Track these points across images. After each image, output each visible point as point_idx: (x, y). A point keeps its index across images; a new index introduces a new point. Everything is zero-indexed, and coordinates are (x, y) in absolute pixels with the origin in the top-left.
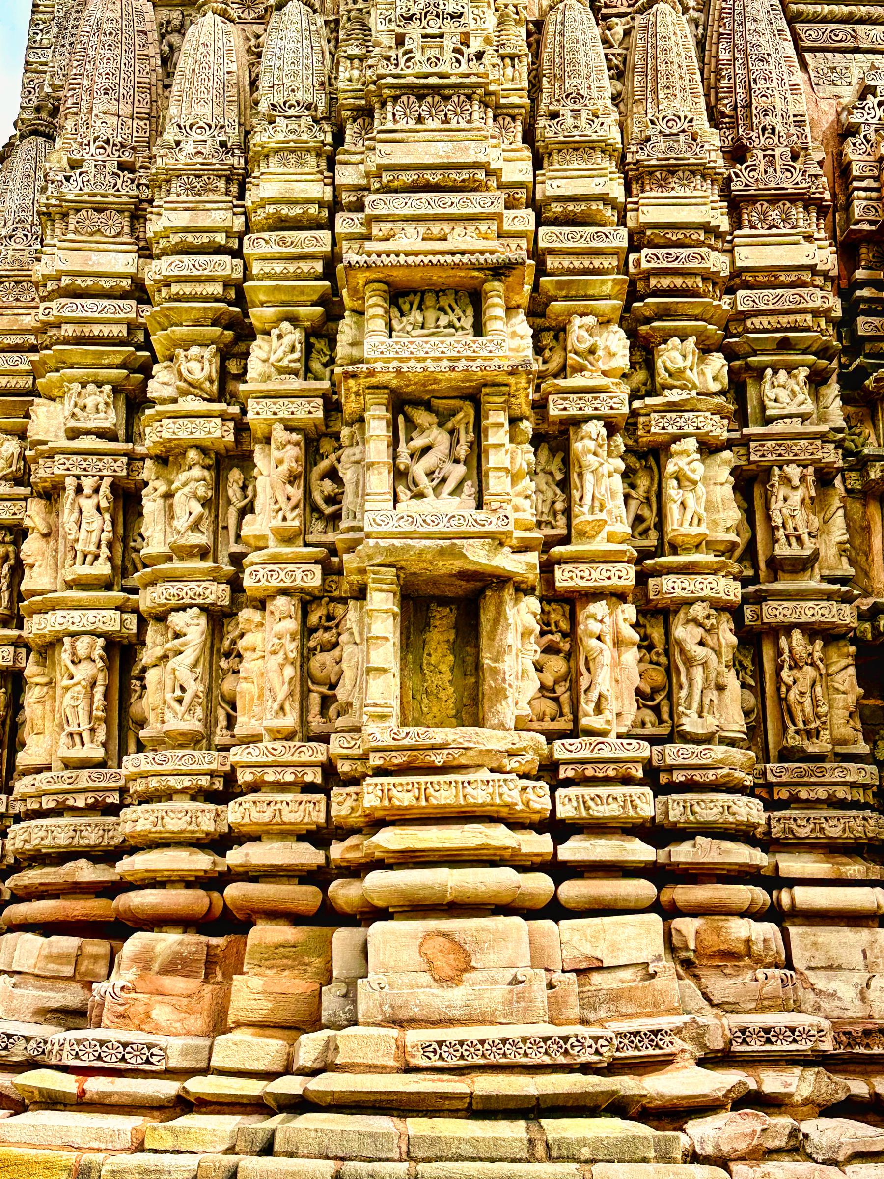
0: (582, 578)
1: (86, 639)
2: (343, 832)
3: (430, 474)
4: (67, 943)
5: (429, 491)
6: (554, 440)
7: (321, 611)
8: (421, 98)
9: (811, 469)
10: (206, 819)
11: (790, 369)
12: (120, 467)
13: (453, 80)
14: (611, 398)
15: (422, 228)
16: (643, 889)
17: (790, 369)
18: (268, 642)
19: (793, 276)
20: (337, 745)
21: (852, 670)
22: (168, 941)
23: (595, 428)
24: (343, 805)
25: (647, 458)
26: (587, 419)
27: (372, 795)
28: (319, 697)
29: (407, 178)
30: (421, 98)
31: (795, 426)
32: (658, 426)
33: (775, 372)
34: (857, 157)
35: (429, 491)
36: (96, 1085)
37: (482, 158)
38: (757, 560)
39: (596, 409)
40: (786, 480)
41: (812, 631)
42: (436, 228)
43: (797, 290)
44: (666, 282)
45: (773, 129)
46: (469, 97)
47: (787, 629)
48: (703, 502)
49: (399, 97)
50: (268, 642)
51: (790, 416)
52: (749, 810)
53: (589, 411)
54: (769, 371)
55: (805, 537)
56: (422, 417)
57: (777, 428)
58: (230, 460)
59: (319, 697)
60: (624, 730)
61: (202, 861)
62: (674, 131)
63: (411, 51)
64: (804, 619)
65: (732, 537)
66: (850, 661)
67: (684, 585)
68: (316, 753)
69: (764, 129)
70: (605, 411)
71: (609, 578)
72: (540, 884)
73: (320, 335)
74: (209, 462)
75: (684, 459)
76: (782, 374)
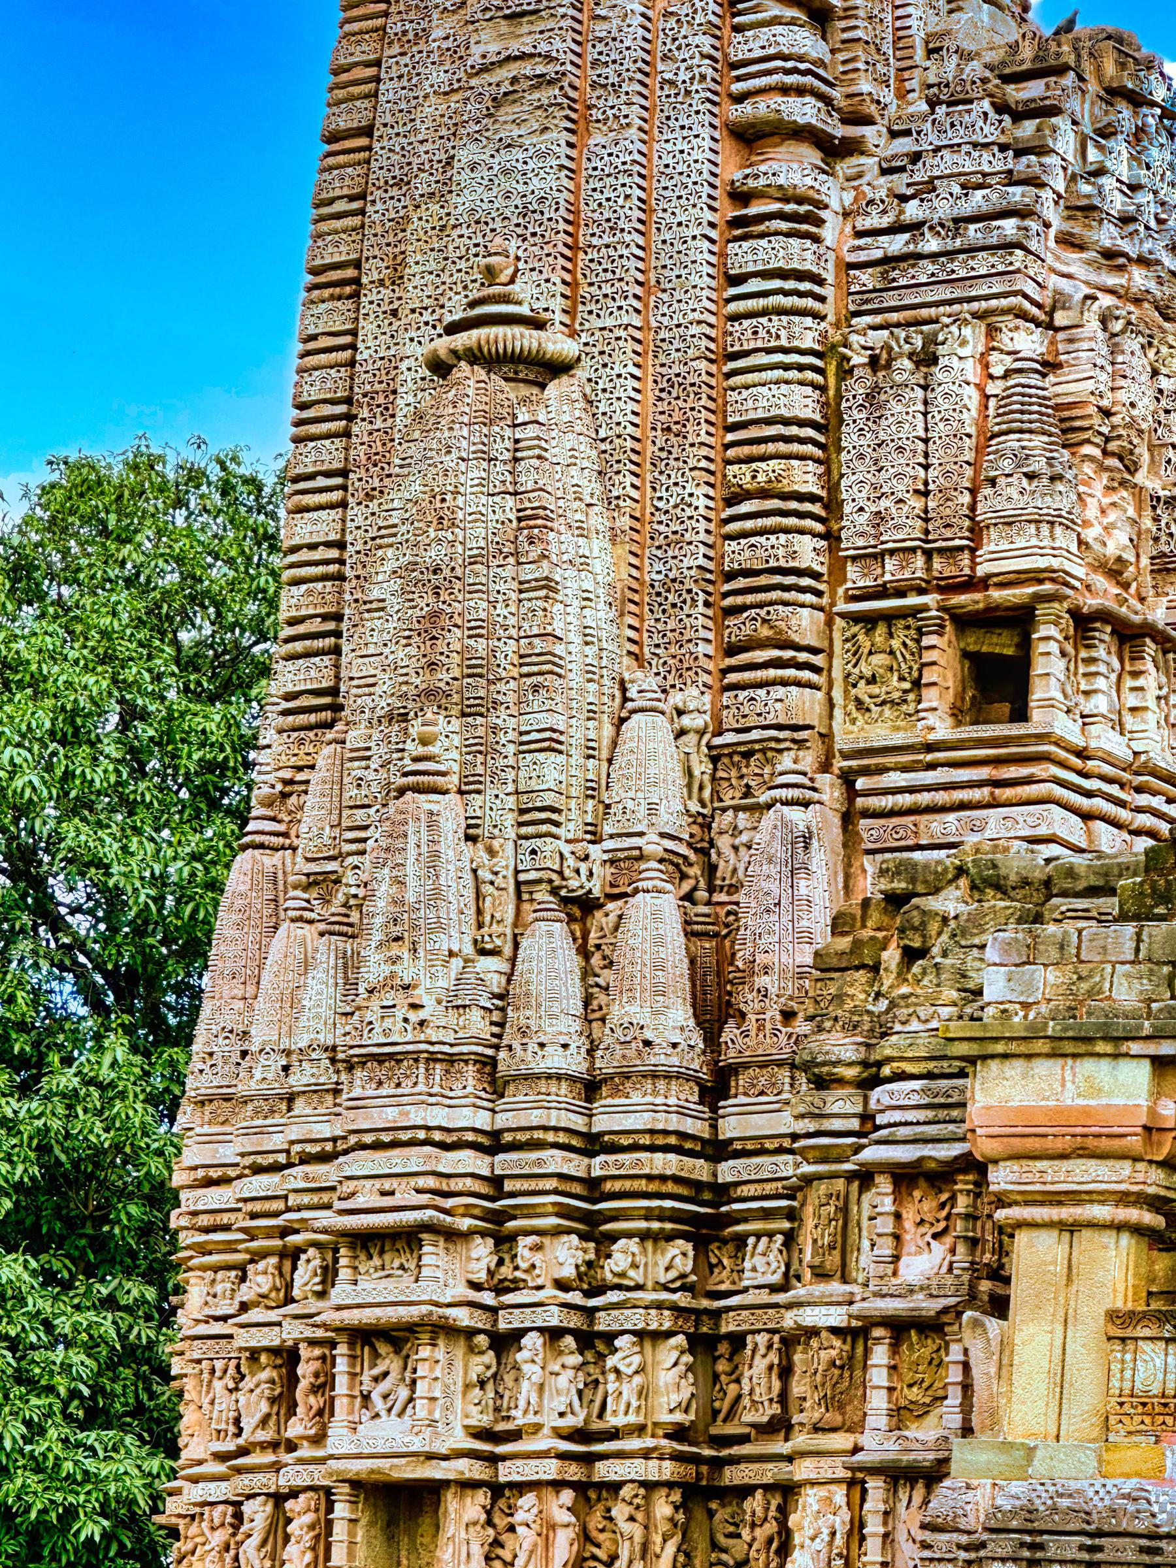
1: (221, 1508)
3: (385, 1397)
5: (383, 1413)
8: (381, 1062)
9: (776, 1338)
15: (378, 1184)
17: (771, 1235)
30: (381, 1062)
32: (603, 1323)
35: (383, 1413)
42: (387, 1185)
46: (416, 1060)
47: (746, 1491)
53: (528, 1324)
54: (751, 1241)
56: (383, 1348)
65: (678, 1417)
74: (279, 1362)
76: (764, 1240)
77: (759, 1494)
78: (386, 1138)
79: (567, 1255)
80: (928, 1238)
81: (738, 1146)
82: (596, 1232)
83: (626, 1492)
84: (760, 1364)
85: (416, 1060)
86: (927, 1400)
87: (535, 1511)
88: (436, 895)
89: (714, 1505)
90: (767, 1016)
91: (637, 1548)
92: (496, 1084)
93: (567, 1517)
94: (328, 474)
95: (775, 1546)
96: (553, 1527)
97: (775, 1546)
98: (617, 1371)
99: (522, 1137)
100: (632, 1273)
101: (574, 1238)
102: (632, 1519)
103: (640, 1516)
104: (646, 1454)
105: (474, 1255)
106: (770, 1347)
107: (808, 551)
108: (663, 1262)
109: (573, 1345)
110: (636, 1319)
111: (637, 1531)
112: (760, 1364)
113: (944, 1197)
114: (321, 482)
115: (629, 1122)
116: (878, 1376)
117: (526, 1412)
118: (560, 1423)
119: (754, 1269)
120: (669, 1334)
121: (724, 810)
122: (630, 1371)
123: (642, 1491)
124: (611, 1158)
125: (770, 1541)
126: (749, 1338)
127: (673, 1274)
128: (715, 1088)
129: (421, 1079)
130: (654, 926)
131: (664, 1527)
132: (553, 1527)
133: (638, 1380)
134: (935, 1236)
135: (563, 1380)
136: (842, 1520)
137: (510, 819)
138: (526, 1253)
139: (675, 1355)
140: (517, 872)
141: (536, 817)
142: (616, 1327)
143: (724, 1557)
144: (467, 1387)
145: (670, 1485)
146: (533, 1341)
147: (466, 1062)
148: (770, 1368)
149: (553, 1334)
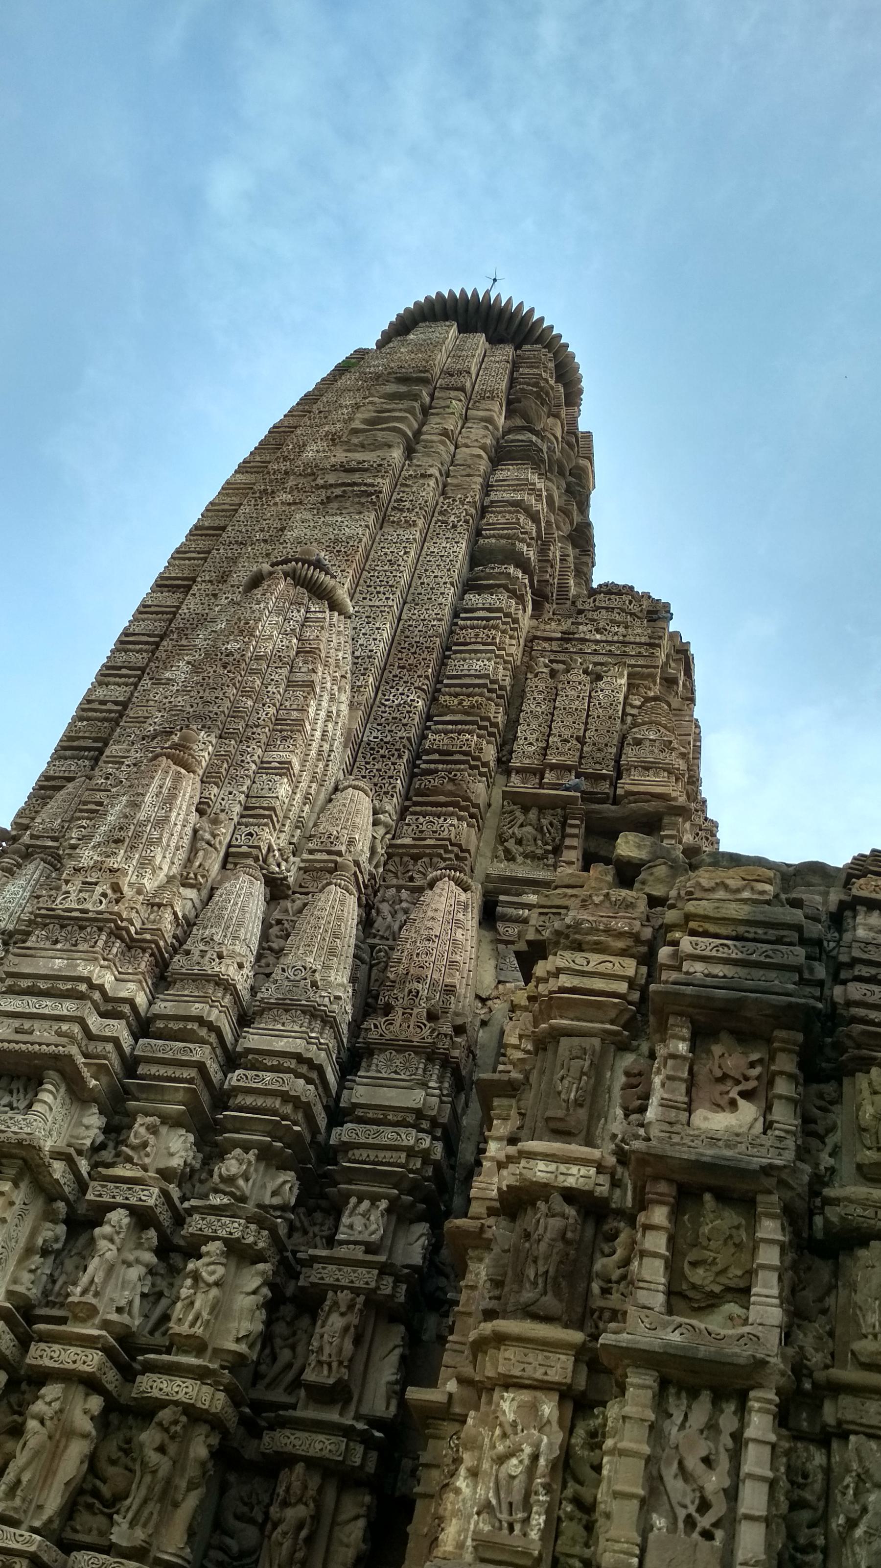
0: (52, 1358)
9: (362, 1298)
11: (375, 1199)
13: (90, 915)
14: (143, 1190)
15: (17, 1023)
17: (375, 1199)
19: (399, 1117)
21: (361, 1523)
23: (118, 1217)
26: (112, 1207)
29: (25, 983)
31: (359, 1253)
33: (360, 1201)
37: (85, 973)
39: (127, 1199)
40: (336, 1304)
41: (312, 1463)
43: (396, 1129)
44: (249, 1100)
45: (418, 992)
48: (223, 1305)
49: (47, 925)
51: (356, 1243)
53: (119, 1199)
54: (353, 1200)
55: (335, 1365)
57: (342, 1252)
60: (37, 1524)
62: (297, 978)
63: (68, 892)
64: (311, 1453)
65: (243, 1348)
66: (363, 1511)
67: (161, 1386)
69: (410, 992)
70: (133, 1201)
71: (75, 1362)
76: (366, 1204)
77: (300, 1468)
78: (43, 985)
79: (178, 1148)
80: (734, 1094)
81: (359, 1112)
82: (210, 1143)
83: (165, 1415)
84: (336, 1322)
85: (100, 929)
86: (717, 1289)
87: (56, 1405)
88: (162, 822)
89: (232, 1478)
90: (416, 1011)
91: (158, 1488)
92: (162, 978)
93: (86, 1425)
94: (130, 668)
95: (304, 1533)
96: (70, 1433)
97: (304, 1533)
98: (196, 1277)
99: (174, 1026)
100: (241, 1182)
101: (191, 1138)
102: (161, 1449)
103: (172, 1449)
104: (201, 1375)
105: (86, 1121)
106: (351, 1307)
107: (490, 753)
108: (271, 1186)
109: (155, 1242)
110: (233, 1227)
111: (164, 1465)
112: (336, 1322)
113: (755, 1057)
114: (124, 671)
115: (280, 1045)
116: (657, 1242)
117: (84, 1292)
118: (114, 1317)
119: (351, 1227)
120: (259, 1258)
121: (388, 887)
122: (211, 1279)
123: (184, 1419)
124: (251, 1073)
125: (300, 1526)
126: (330, 1294)
127: (276, 1201)
128: (352, 1060)
129: (100, 943)
130: (338, 909)
131: (193, 1471)
132: (70, 1433)
133: (214, 1292)
134: (744, 1095)
135: (134, 1273)
136: (550, 1443)
137: (237, 809)
138: (142, 1130)
139: (256, 1282)
140: (230, 845)
141: (256, 812)
142: (208, 1232)
143: (228, 1541)
144: (29, 1251)
145: (213, 1422)
146: (118, 1217)
147: (144, 951)
148: (346, 1329)
149: (142, 1218)
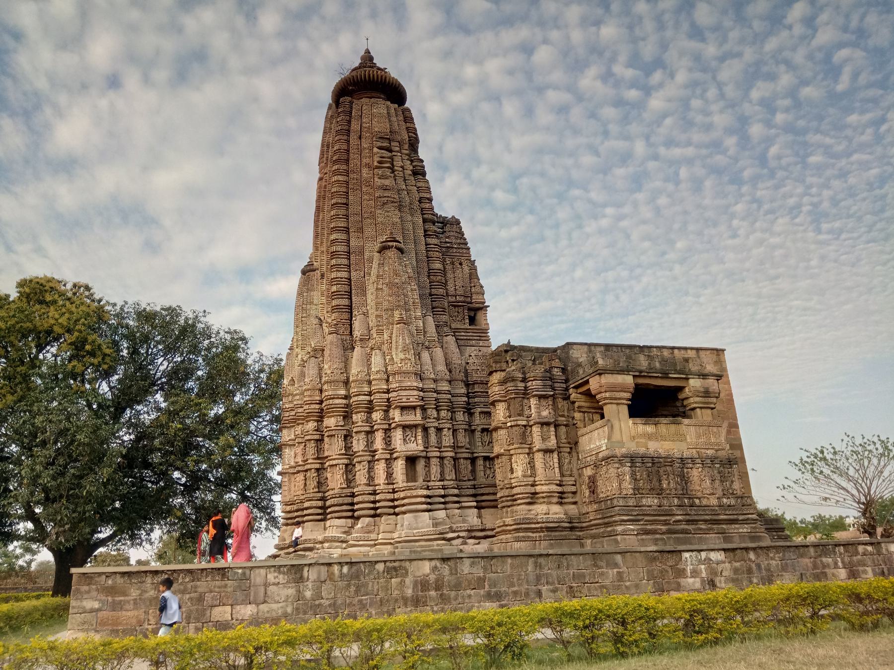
2: (397, 500)
4: (343, 520)
6: (425, 429)
7: (389, 462)
10: (372, 498)
12: (345, 432)
16: (442, 506)
18: (380, 469)
20: (395, 486)
22: (368, 520)
24: (396, 496)
25: (439, 430)
27: (402, 495)
28: (389, 475)
34: (469, 368)
36: (361, 543)
38: (455, 447)
48: (447, 439)
50: (380, 469)
52: (456, 491)
58: (370, 433)
59: (389, 475)
61: (372, 505)
68: (391, 487)
72: (429, 507)
73: (386, 412)
75: (445, 432)
